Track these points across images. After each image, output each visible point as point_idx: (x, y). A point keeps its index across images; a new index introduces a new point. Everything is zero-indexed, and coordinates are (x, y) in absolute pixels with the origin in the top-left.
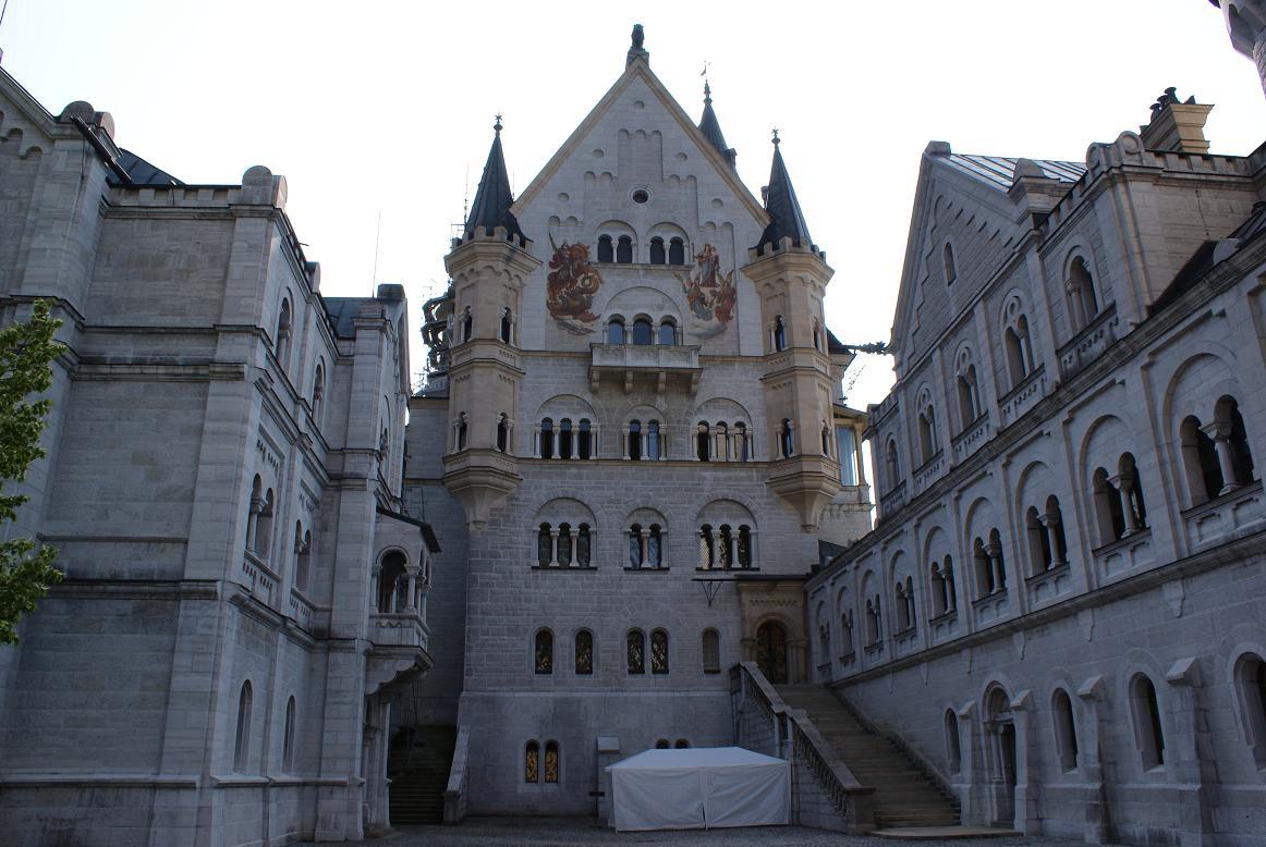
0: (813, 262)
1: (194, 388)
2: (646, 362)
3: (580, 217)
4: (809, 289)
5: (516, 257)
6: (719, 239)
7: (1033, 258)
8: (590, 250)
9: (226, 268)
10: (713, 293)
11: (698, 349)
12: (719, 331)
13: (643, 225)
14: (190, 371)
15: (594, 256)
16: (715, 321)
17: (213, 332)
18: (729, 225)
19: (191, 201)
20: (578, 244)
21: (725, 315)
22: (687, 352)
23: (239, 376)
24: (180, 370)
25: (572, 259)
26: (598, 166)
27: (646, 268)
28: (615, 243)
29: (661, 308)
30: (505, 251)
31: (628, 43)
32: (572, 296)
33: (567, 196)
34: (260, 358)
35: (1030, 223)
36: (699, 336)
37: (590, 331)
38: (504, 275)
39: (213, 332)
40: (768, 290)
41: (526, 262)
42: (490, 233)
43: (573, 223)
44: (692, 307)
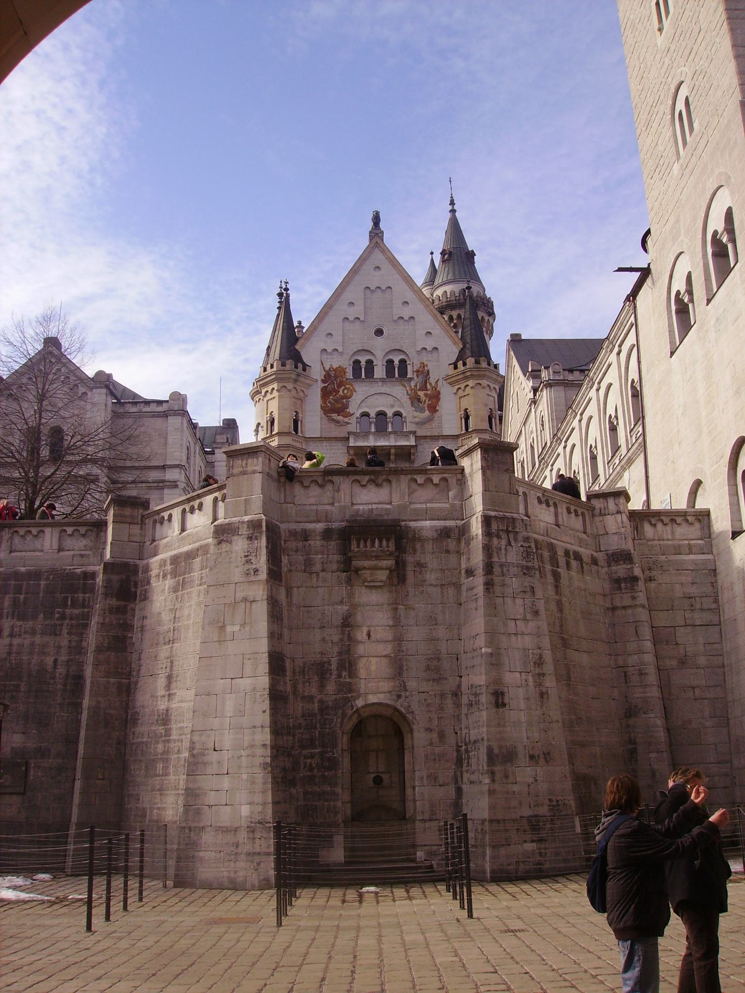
0: (487, 373)
1: (158, 492)
2: (382, 443)
3: (340, 349)
4: (487, 391)
5: (301, 379)
6: (430, 359)
7: (533, 410)
8: (347, 370)
9: (166, 438)
10: (426, 395)
11: (414, 433)
12: (430, 420)
13: (380, 350)
14: (156, 485)
15: (349, 374)
16: (427, 413)
17: (164, 467)
18: (436, 348)
19: (147, 409)
20: (340, 367)
21: (433, 409)
22: (407, 435)
23: (176, 486)
24: (152, 485)
25: (336, 377)
26: (352, 313)
27: (382, 380)
28: (363, 363)
29: (392, 406)
30: (293, 376)
31: (371, 225)
32: (337, 401)
33: (330, 334)
34: (183, 478)
35: (531, 395)
36: (417, 423)
37: (348, 423)
38: (294, 391)
39: (164, 467)
40: (460, 391)
41: (306, 381)
42: (283, 365)
43: (336, 353)
44: (412, 404)
